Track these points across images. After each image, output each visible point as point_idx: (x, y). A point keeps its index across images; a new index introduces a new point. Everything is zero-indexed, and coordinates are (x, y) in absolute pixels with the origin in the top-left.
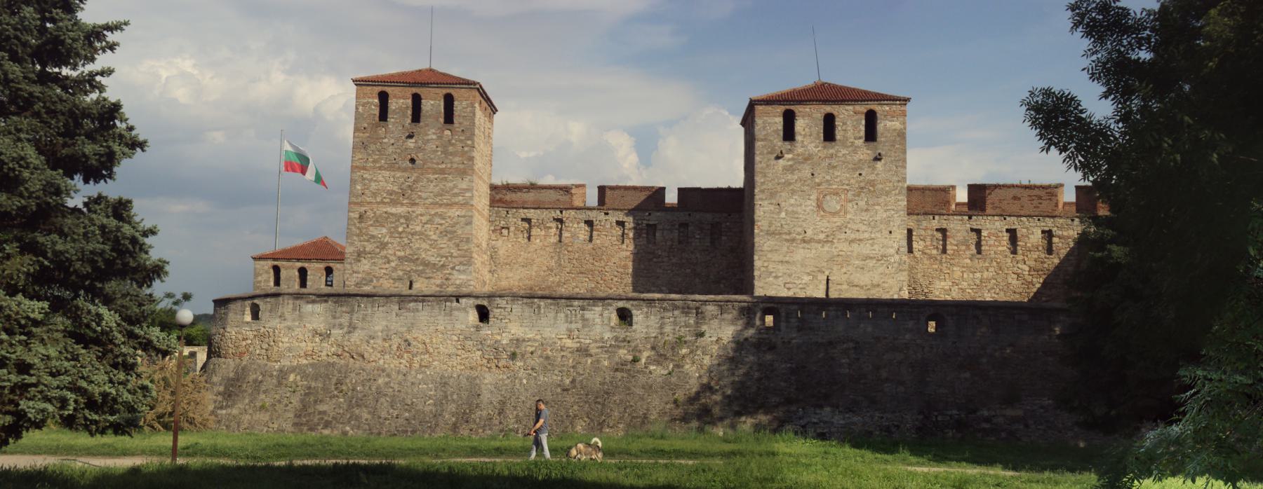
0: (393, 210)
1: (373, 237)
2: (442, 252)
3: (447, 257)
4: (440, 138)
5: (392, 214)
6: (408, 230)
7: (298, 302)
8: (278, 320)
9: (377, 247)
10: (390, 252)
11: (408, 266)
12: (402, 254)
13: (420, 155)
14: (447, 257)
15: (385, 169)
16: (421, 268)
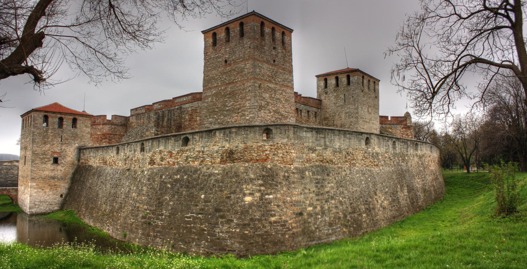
0: (270, 85)
1: (264, 98)
2: (287, 110)
3: (288, 113)
4: (282, 52)
5: (270, 88)
6: (275, 97)
7: (296, 129)
8: (286, 140)
9: (266, 104)
10: (271, 107)
11: (277, 116)
12: (274, 109)
13: (277, 59)
14: (288, 113)
15: (266, 63)
16: (280, 117)
